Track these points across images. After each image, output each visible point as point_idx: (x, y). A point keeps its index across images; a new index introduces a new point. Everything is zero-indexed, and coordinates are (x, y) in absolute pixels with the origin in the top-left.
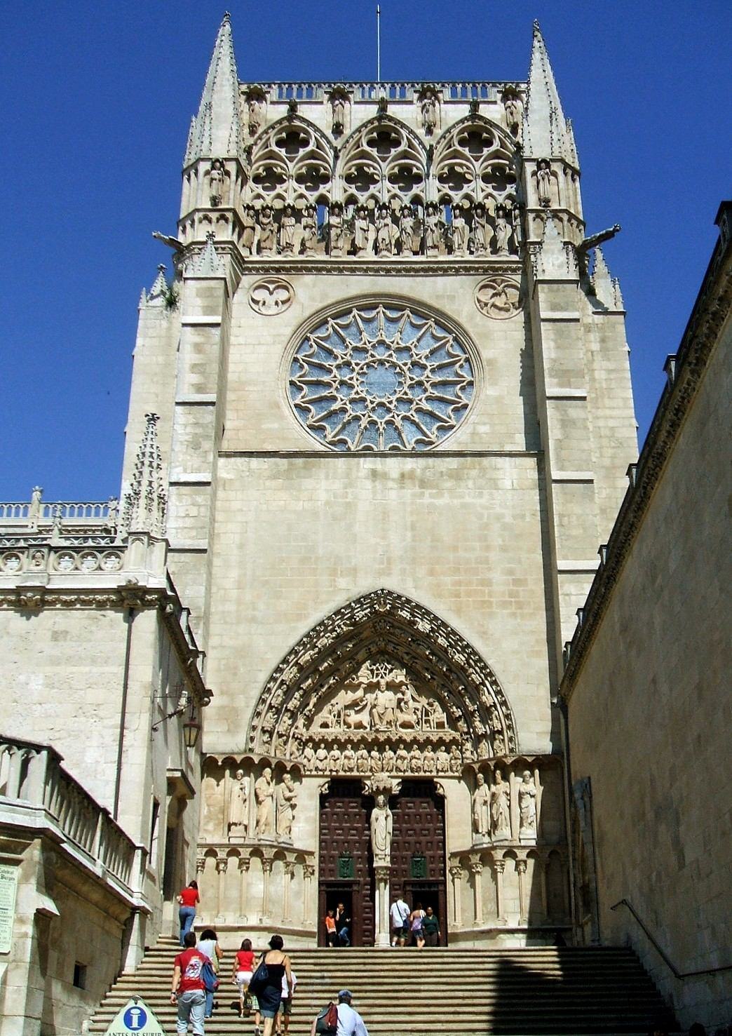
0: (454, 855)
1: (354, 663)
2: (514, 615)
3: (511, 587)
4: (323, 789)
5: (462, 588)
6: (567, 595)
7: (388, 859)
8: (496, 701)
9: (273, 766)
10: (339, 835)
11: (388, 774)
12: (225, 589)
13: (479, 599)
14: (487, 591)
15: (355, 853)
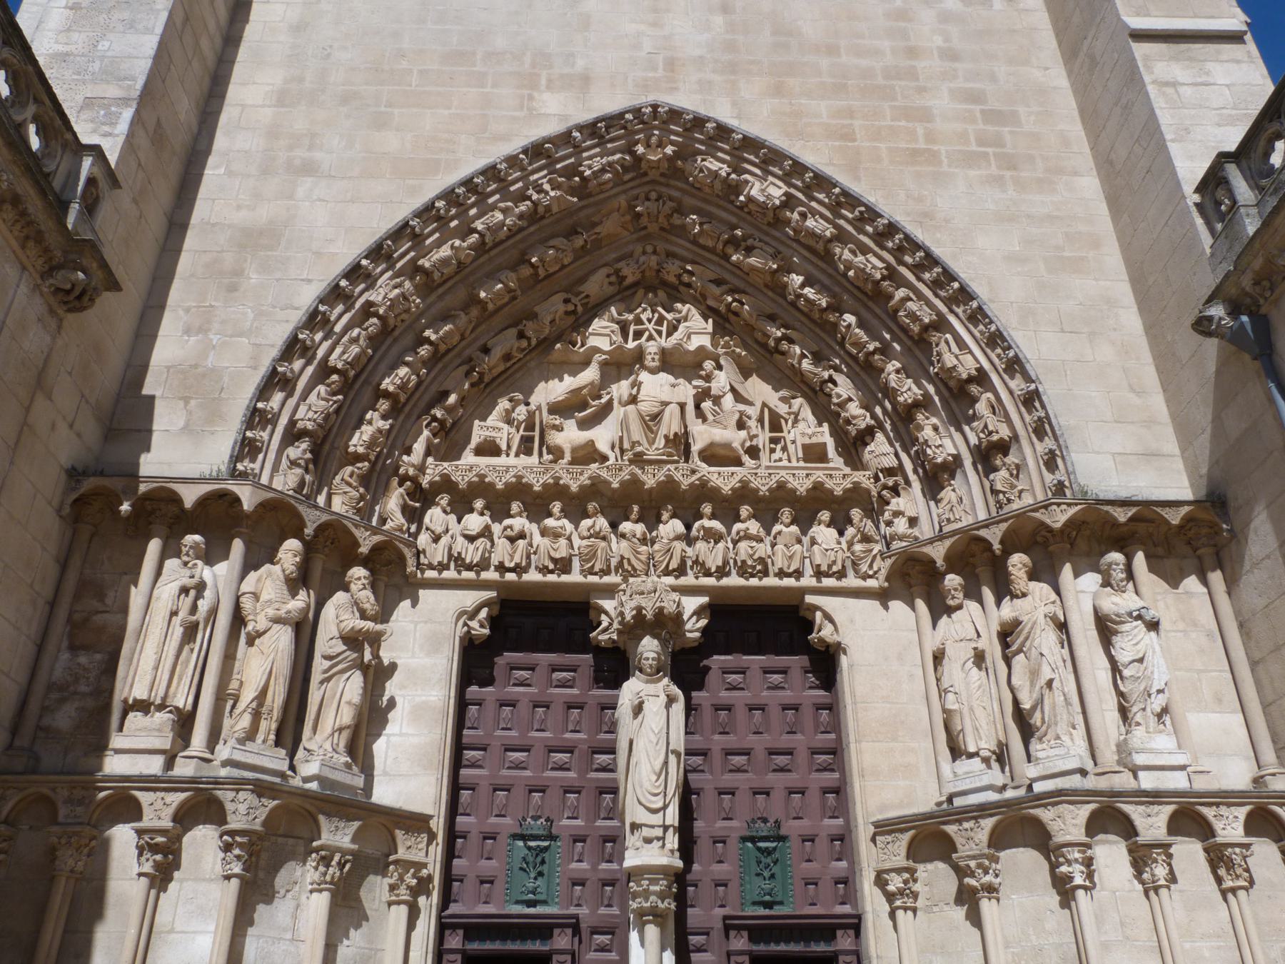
0: (884, 828)
1: (575, 300)
2: (998, 181)
3: (981, 126)
4: (474, 624)
5: (857, 123)
6: (1167, 84)
7: (673, 841)
8: (986, 365)
9: (309, 531)
10: (518, 766)
11: (670, 580)
12: (243, 106)
13: (903, 145)
14: (920, 131)
15: (565, 822)
